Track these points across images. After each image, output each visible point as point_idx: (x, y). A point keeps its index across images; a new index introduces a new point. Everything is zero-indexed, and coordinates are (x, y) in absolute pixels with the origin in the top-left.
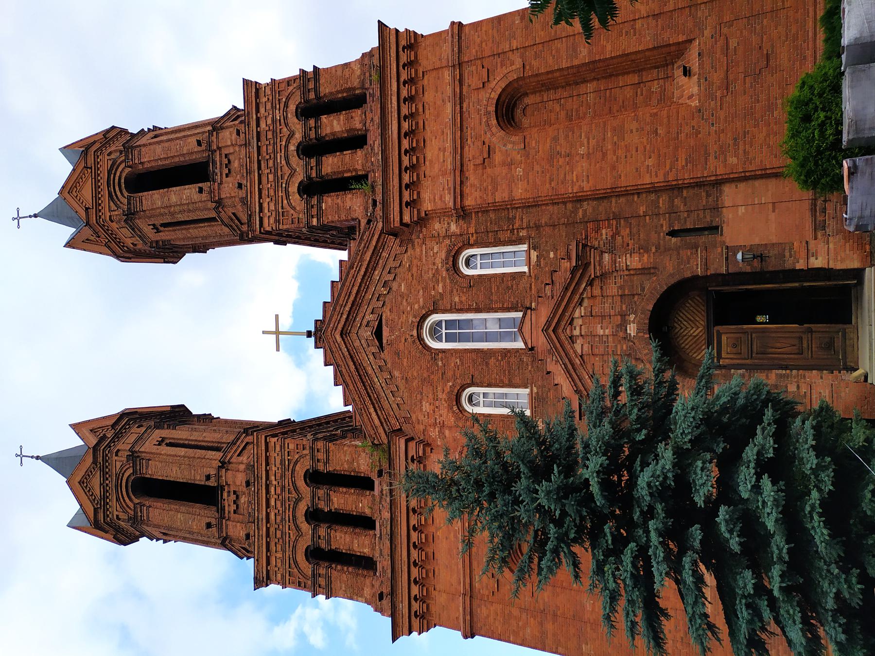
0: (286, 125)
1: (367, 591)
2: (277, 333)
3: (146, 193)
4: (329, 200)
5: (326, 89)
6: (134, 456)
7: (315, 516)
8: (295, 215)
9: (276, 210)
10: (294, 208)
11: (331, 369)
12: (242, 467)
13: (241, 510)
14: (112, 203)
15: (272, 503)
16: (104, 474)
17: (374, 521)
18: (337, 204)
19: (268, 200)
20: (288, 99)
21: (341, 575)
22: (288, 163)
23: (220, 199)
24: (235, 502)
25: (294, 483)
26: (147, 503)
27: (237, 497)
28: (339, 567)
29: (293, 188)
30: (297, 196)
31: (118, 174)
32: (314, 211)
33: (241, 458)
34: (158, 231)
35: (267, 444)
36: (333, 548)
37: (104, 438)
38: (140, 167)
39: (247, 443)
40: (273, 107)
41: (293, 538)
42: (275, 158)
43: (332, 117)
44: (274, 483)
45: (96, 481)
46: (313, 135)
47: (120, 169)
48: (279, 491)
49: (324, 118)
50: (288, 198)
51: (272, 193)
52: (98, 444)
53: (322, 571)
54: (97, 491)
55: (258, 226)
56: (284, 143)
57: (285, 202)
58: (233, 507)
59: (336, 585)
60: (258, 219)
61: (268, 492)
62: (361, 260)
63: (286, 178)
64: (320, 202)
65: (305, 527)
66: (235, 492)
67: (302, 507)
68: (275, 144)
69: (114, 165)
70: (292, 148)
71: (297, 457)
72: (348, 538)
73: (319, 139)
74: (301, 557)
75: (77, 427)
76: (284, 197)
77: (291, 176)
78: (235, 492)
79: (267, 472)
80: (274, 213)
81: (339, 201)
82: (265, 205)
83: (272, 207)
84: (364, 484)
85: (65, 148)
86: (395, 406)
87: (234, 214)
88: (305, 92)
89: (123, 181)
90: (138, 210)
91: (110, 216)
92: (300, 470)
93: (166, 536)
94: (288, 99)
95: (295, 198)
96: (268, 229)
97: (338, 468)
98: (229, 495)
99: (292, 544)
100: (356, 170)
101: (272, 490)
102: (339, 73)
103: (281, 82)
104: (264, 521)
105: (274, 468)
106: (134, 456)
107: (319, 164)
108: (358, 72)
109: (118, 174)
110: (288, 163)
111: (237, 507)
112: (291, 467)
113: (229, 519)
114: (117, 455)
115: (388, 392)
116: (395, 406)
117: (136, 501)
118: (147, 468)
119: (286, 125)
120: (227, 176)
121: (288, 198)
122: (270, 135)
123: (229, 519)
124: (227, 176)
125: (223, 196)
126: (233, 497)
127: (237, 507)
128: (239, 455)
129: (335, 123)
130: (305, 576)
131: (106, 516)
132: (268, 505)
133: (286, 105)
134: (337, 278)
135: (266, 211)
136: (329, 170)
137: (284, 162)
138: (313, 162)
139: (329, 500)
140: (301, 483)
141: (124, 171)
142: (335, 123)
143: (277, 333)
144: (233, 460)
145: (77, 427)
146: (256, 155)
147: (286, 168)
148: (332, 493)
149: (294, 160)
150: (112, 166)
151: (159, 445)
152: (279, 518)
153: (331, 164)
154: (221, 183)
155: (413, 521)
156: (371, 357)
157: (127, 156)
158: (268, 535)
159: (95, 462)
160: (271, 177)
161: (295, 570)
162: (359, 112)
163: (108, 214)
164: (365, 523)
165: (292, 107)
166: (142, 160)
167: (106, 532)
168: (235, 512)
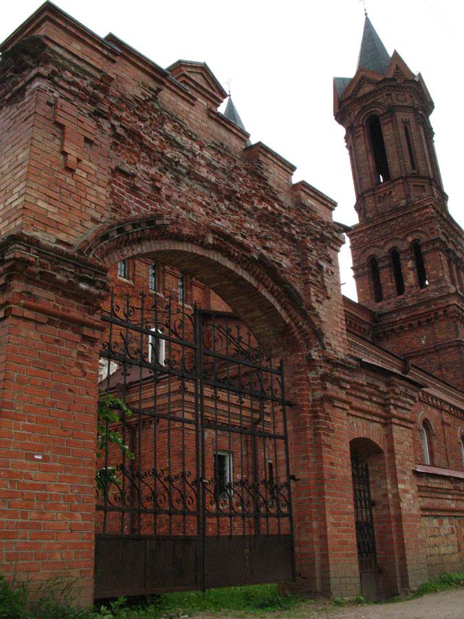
6: (391, 110)
7: (395, 255)
17: (402, 294)
24: (385, 194)
36: (381, 272)
39: (423, 186)
45: (367, 89)
52: (388, 79)
53: (366, 269)
54: (361, 94)
65: (386, 250)
67: (396, 243)
75: (396, 54)
93: (351, 147)
114: (387, 95)
128: (414, 185)
131: (348, 106)
145: (396, 54)
151: (403, 122)
159: (378, 83)
167: (339, 107)
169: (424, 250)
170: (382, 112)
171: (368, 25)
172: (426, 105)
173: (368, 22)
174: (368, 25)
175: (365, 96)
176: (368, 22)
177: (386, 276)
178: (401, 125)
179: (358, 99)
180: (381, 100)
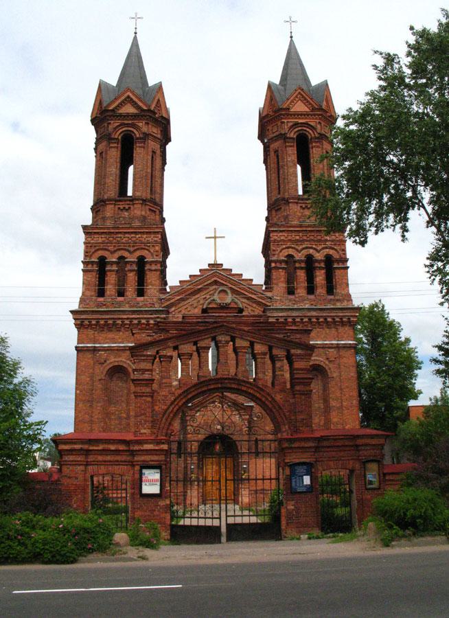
0: (323, 248)
1: (88, 293)
2: (215, 238)
3: (295, 148)
4: (283, 274)
5: (338, 273)
8: (277, 252)
9: (280, 241)
10: (281, 251)
11: (198, 273)
12: (143, 213)
13: (120, 212)
14: (291, 124)
15: (126, 236)
16: (134, 116)
18: (280, 278)
19: (286, 235)
20: (336, 250)
21: (94, 278)
22: (304, 249)
23: (289, 203)
24: (124, 208)
25: (138, 249)
26: (119, 145)
27: (127, 210)
28: (97, 276)
29: (291, 252)
30: (286, 254)
31: (308, 130)
32: (278, 265)
33: (148, 212)
34: (275, 152)
35: (158, 232)
36: (108, 273)
37: (155, 113)
38: (310, 146)
40: (332, 241)
41: (110, 248)
42: (307, 241)
43: (324, 276)
44: (137, 236)
45: (129, 109)
46: (317, 265)
47: (310, 131)
48: (134, 239)
49: (323, 271)
50: (286, 248)
51: (290, 238)
55: (272, 229)
56: (314, 246)
57: (284, 247)
58: (122, 207)
59: (90, 275)
60: (276, 229)
61: (132, 233)
62: (252, 293)
63: (297, 247)
64: (283, 268)
66: (130, 208)
68: (314, 241)
69: (313, 128)
70: (311, 251)
71: (152, 251)
72: (113, 282)
73: (315, 268)
74: (101, 253)
76: (287, 246)
77: (297, 250)
78: (130, 208)
79: (143, 232)
80: (279, 239)
81: (282, 279)
82: (284, 234)
83: (282, 238)
84: (141, 293)
85: (327, 84)
86: (179, 310)
87: (281, 208)
88: (338, 261)
89: (305, 132)
90: (287, 144)
91: (284, 122)
92: (144, 253)
94: (336, 250)
95: (286, 252)
96: (271, 235)
97: (148, 276)
98: (128, 204)
99: (107, 247)
100: (297, 289)
101: (133, 235)
102: (344, 281)
103: (345, 245)
104: (117, 231)
105: (145, 236)
106: (146, 136)
107: (302, 268)
108: (343, 293)
109: (308, 130)
110: (304, 249)
111: (122, 210)
112: (146, 247)
113: (115, 205)
115: (187, 306)
116: (179, 310)
117: (120, 138)
118: (140, 147)
119: (323, 248)
120: (301, 207)
121: (286, 248)
122: (319, 237)
123: (115, 205)
124: (301, 207)
125: (290, 205)
126: (127, 207)
127: (122, 210)
128: (150, 209)
129: (321, 278)
130: (91, 256)
132: (125, 233)
133: (333, 249)
134: (244, 277)
135: (281, 234)
136: (298, 274)
137: (304, 246)
138: (303, 265)
139: (131, 271)
140: (138, 253)
141: (311, 134)
142: (321, 278)
143: (215, 238)
144: (148, 207)
146: (309, 229)
147: (301, 247)
148: (135, 272)
149: (305, 252)
150: (312, 126)
152: (119, 239)
153: (301, 275)
154: (297, 203)
155: (127, 322)
156: (204, 296)
157: (318, 138)
158: (109, 232)
159: (143, 110)
160: (298, 237)
161: (93, 250)
162: (325, 292)
163: (285, 121)
164: (121, 293)
165: (331, 252)
166: (314, 149)
168: (119, 208)
169: (147, 267)
170: (138, 136)
171: (135, 45)
172: (166, 138)
173: (135, 44)
174: (135, 45)
175: (127, 116)
176: (135, 44)
177: (111, 279)
178: (150, 153)
179: (121, 115)
180: (140, 124)
